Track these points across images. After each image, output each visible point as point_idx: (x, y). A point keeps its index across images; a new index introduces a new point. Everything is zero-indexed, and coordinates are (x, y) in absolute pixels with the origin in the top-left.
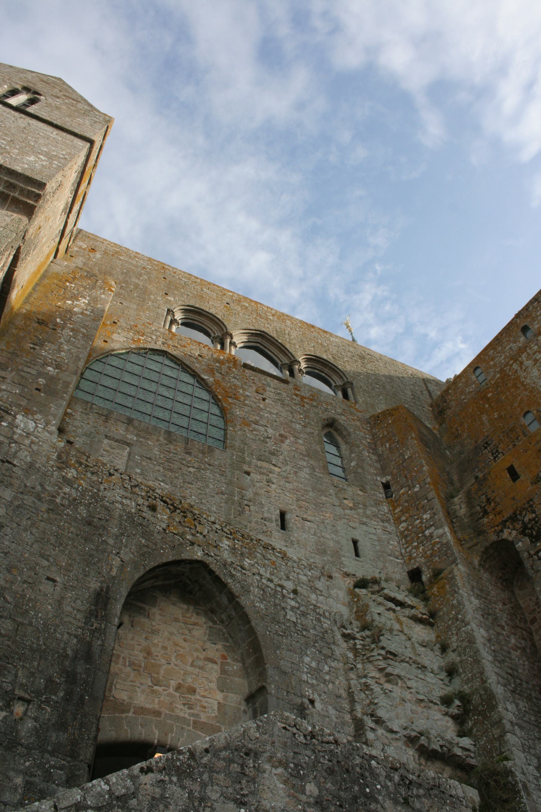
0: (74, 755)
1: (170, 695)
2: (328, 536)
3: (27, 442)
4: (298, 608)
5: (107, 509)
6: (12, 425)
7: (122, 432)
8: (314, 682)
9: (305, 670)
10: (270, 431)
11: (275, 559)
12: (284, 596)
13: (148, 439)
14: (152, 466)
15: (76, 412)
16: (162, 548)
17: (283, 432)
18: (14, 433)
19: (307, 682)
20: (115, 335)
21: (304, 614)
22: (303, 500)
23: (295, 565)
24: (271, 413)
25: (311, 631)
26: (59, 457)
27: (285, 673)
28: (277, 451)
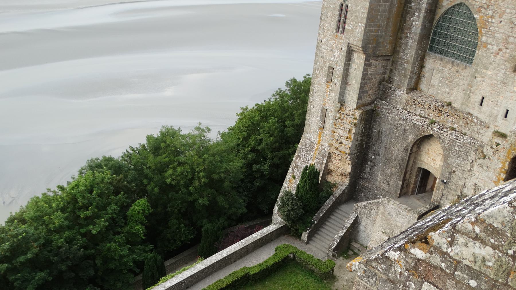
0: (400, 177)
3: (399, 100)
6: (396, 95)
7: (438, 66)
8: (458, 166)
10: (495, 48)
12: (456, 142)
13: (446, 67)
14: (444, 81)
15: (426, 60)
16: (422, 133)
17: (501, 47)
18: (396, 98)
21: (461, 147)
24: (500, 33)
27: (449, 164)
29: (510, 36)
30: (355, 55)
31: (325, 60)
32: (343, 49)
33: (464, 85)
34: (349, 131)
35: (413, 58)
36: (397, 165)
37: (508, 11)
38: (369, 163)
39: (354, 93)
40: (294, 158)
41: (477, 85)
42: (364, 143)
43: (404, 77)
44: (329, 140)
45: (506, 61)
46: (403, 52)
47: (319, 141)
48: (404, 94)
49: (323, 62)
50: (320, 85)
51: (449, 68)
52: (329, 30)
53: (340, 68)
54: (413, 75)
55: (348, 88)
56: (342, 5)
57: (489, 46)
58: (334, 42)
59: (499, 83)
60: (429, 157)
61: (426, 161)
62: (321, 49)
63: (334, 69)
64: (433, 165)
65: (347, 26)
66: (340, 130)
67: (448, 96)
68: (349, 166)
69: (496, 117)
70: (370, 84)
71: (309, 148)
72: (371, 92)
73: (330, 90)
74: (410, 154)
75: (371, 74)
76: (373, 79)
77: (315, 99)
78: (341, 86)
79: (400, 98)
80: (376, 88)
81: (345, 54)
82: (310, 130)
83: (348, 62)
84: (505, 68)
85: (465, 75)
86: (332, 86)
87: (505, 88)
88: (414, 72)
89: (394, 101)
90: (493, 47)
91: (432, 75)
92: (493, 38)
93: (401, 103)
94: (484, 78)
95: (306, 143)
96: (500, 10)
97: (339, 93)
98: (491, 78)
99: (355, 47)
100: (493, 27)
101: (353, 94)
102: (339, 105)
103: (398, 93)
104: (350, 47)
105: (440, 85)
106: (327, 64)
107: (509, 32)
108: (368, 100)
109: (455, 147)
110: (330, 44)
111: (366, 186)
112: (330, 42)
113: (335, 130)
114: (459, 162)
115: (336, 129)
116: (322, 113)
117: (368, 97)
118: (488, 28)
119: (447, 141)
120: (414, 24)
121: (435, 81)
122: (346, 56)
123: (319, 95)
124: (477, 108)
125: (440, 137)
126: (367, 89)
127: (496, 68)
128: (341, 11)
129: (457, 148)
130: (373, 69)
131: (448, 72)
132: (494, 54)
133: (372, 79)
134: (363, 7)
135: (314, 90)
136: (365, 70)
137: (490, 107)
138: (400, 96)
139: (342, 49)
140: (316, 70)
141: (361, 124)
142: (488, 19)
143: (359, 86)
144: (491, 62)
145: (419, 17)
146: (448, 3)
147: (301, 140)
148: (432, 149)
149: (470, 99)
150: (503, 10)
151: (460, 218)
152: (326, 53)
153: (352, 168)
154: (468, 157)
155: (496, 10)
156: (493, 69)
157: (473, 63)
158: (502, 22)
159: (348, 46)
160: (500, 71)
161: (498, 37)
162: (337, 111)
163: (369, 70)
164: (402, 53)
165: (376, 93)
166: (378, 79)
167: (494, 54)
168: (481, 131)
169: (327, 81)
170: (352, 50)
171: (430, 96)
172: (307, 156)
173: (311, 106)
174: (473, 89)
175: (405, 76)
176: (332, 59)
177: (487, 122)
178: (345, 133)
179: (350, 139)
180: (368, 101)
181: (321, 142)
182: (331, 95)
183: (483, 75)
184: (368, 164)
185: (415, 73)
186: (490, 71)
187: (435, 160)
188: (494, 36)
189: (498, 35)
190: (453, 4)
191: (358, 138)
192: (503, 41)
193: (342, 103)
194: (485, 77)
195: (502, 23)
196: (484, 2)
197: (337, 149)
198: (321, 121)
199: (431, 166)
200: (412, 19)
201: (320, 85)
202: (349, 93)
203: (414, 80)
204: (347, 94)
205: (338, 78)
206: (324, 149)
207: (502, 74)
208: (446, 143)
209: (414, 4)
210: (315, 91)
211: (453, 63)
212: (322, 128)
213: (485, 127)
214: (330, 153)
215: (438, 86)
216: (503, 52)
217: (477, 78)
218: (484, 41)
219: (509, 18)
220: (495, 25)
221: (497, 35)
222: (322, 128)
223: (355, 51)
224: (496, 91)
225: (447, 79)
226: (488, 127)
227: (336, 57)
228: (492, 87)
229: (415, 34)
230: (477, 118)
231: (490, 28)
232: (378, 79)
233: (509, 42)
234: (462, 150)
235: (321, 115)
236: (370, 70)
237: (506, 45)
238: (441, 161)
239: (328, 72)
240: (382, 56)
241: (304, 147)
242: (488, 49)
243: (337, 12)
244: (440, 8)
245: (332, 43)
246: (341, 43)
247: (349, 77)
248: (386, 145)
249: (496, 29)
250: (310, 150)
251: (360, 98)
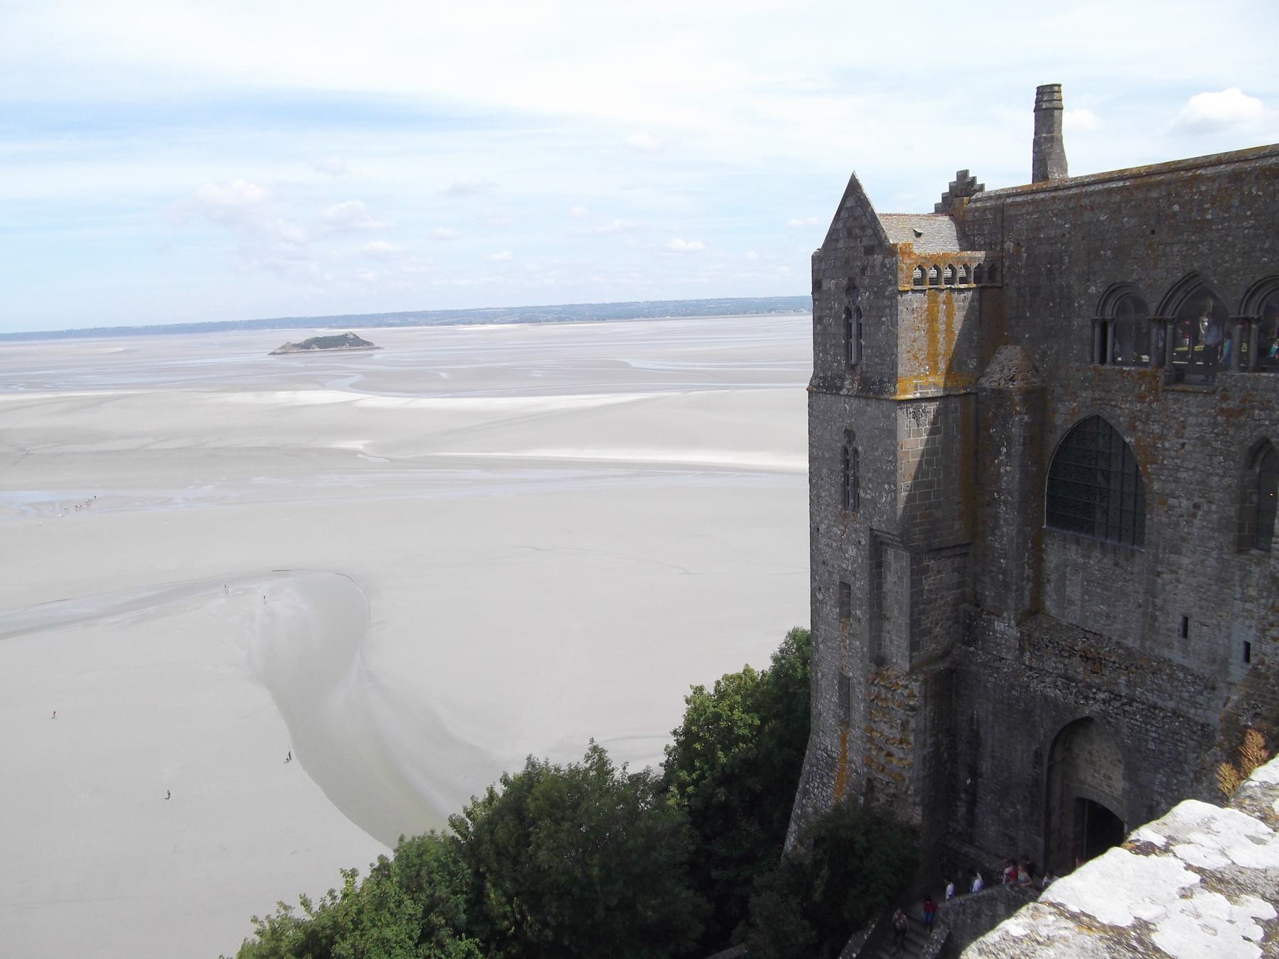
1: (1100, 779)
2: (1220, 642)
3: (1003, 641)
4: (1158, 738)
5: (1032, 697)
6: (995, 632)
8: (1164, 791)
9: (1157, 783)
10: (1184, 503)
11: (1161, 682)
12: (1147, 730)
17: (1196, 500)
19: (1158, 791)
20: (1056, 415)
21: (1162, 742)
22: (1205, 599)
23: (1180, 684)
24: (1188, 469)
25: (1168, 755)
26: (1020, 645)
28: (1189, 534)
29: (1211, 474)
30: (889, 552)
31: (831, 569)
32: (862, 543)
33: (1138, 593)
34: (902, 724)
35: (1015, 545)
36: (1025, 797)
37: (1192, 420)
38: (963, 796)
39: (901, 638)
40: (798, 796)
41: (1164, 590)
42: (943, 748)
43: (1004, 589)
44: (864, 749)
45: (1213, 530)
46: (993, 535)
47: (845, 751)
48: (1012, 628)
49: (827, 574)
50: (829, 625)
51: (1097, 557)
52: (828, 505)
53: (862, 583)
54: (1024, 583)
55: (887, 626)
56: (846, 451)
57: (1172, 501)
58: (843, 528)
59: (1211, 582)
60: (1095, 771)
61: (1089, 779)
62: (819, 546)
63: (852, 588)
64: (1107, 790)
65: (862, 495)
66: (882, 724)
67: (1108, 622)
68: (917, 808)
69: (1225, 662)
70: (932, 614)
71: (826, 770)
72: (938, 629)
73: (850, 634)
74: (1050, 768)
75: (930, 591)
76: (939, 601)
77: (823, 657)
78: (870, 624)
79: (1005, 636)
80: (948, 619)
81: (867, 552)
82: (823, 727)
83: (876, 568)
84: (1215, 545)
85: (1136, 570)
86: (851, 625)
87: (1229, 591)
88: (1025, 576)
89: (992, 645)
90: (1180, 503)
91: (1066, 577)
92: (1174, 481)
93: (1009, 648)
94: (1176, 572)
95: (817, 758)
96: (1174, 421)
97: (868, 640)
98: (1192, 573)
99: (887, 536)
100: (1170, 458)
101: (898, 639)
102: (873, 668)
103: (999, 626)
104: (876, 536)
105: (1087, 597)
106: (836, 577)
107: (1205, 465)
108: (934, 649)
109: (1147, 743)
110: (836, 534)
111: (964, 855)
112: (835, 529)
113: (873, 725)
114: (1164, 779)
115: (875, 722)
116: (840, 688)
117: (934, 641)
118: (1159, 462)
119: (1125, 730)
120: (1002, 471)
121: (1074, 591)
122: (871, 558)
123: (829, 648)
124: (1176, 644)
125: (1108, 720)
126: (929, 625)
127: (1198, 548)
128: (846, 462)
129: (1152, 746)
130: (933, 580)
131: (1096, 568)
132: (1185, 518)
133: (935, 600)
134: (886, 451)
135: (817, 637)
136: (915, 585)
137: (1207, 639)
138: (1003, 633)
139: (860, 542)
140: (817, 593)
141: (926, 706)
142: (1155, 443)
143: (908, 622)
144: (1184, 535)
145: (1008, 454)
146: (1065, 420)
147: (807, 752)
148: (1098, 752)
149: (1156, 624)
150: (1182, 419)
151: (1142, 951)
152: (830, 553)
153: (923, 810)
154: (1184, 765)
155: (1166, 423)
156: (1191, 551)
157: (1146, 543)
158: (1186, 446)
159: (871, 535)
160: (1207, 553)
161: (1184, 478)
162: (870, 682)
163: (924, 582)
164: (991, 536)
165: (951, 630)
166: (949, 599)
167: (1185, 518)
168: (1200, 699)
169: (841, 615)
170: (882, 543)
171: (1070, 627)
172: (822, 789)
173: (816, 673)
174: (1159, 601)
175: (1006, 586)
176: (844, 565)
177: (1207, 676)
178: (894, 731)
179: (908, 743)
180: (937, 652)
181: (847, 754)
182: (853, 646)
183: (1174, 568)
184: (961, 799)
185: (1028, 577)
186: (1185, 556)
187: (1110, 778)
188: (1177, 477)
189: (1185, 475)
190: (1077, 419)
191: (925, 740)
192: (1198, 487)
193: (880, 661)
194: (1180, 571)
195: (1187, 447)
196: (1138, 409)
197: (883, 770)
198: (841, 706)
199: (1106, 793)
200: (997, 461)
201: (829, 625)
202: (890, 638)
203: (1027, 593)
204: (887, 640)
205: (861, 606)
206: (857, 772)
207: (1214, 561)
208: (1124, 735)
209: (994, 430)
210: (820, 640)
211: (1102, 545)
212: (845, 723)
213: (1206, 687)
214: (869, 781)
215: (1082, 601)
216: (1203, 511)
217: (1161, 575)
218: (1158, 491)
219: (1198, 435)
220: (1173, 453)
221: (1183, 475)
222: (845, 723)
223: (888, 545)
224: (1210, 601)
225: (1098, 583)
226: (1213, 688)
227: (851, 561)
228: (1199, 592)
229: (1010, 493)
230: (1183, 668)
231: (1162, 462)
232: (949, 599)
233: (1211, 487)
234: (1164, 748)
235: (840, 693)
236: (928, 583)
237: (1206, 496)
238: (1124, 778)
239: (840, 594)
240: (949, 547)
241: (815, 769)
242: (1172, 508)
243: (839, 465)
244: (1051, 432)
245: (839, 532)
246: (856, 530)
247: (884, 602)
248: (993, 751)
249: (1177, 464)
250: (828, 774)
251: (914, 646)
